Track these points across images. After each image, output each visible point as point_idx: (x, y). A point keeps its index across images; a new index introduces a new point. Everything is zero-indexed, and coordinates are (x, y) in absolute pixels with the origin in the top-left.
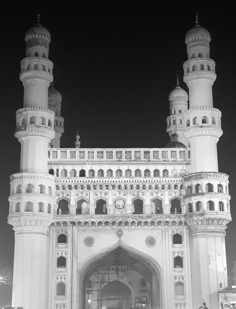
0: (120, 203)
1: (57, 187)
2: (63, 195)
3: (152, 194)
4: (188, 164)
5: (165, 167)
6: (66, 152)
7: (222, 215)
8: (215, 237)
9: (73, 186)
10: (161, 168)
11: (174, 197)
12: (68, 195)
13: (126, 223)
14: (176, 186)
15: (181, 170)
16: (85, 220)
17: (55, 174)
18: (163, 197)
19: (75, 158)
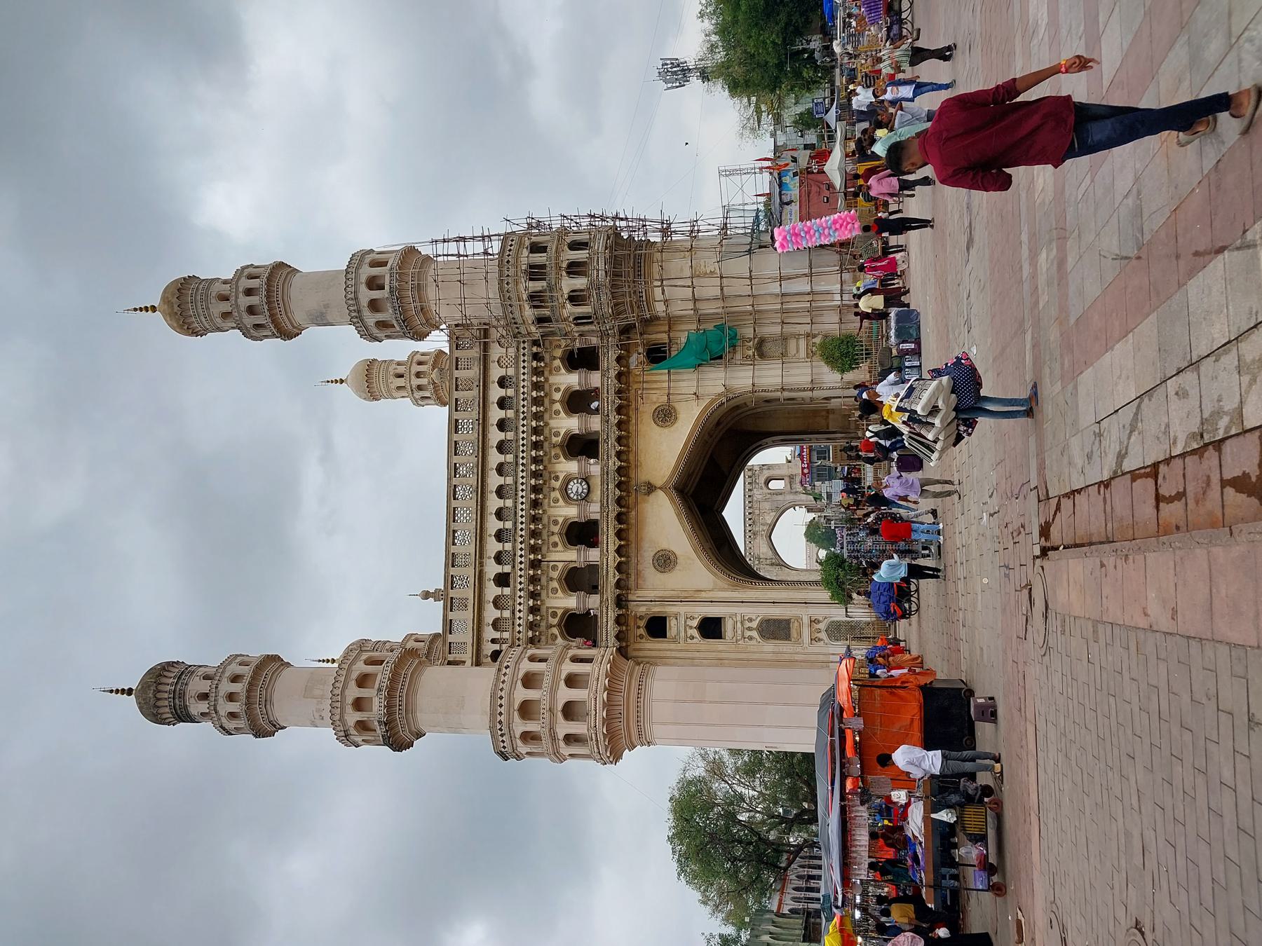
0: (575, 488)
1: (532, 641)
3: (557, 413)
9: (531, 602)
10: (496, 393)
12: (554, 615)
14: (536, 357)
16: (611, 570)
17: (504, 647)
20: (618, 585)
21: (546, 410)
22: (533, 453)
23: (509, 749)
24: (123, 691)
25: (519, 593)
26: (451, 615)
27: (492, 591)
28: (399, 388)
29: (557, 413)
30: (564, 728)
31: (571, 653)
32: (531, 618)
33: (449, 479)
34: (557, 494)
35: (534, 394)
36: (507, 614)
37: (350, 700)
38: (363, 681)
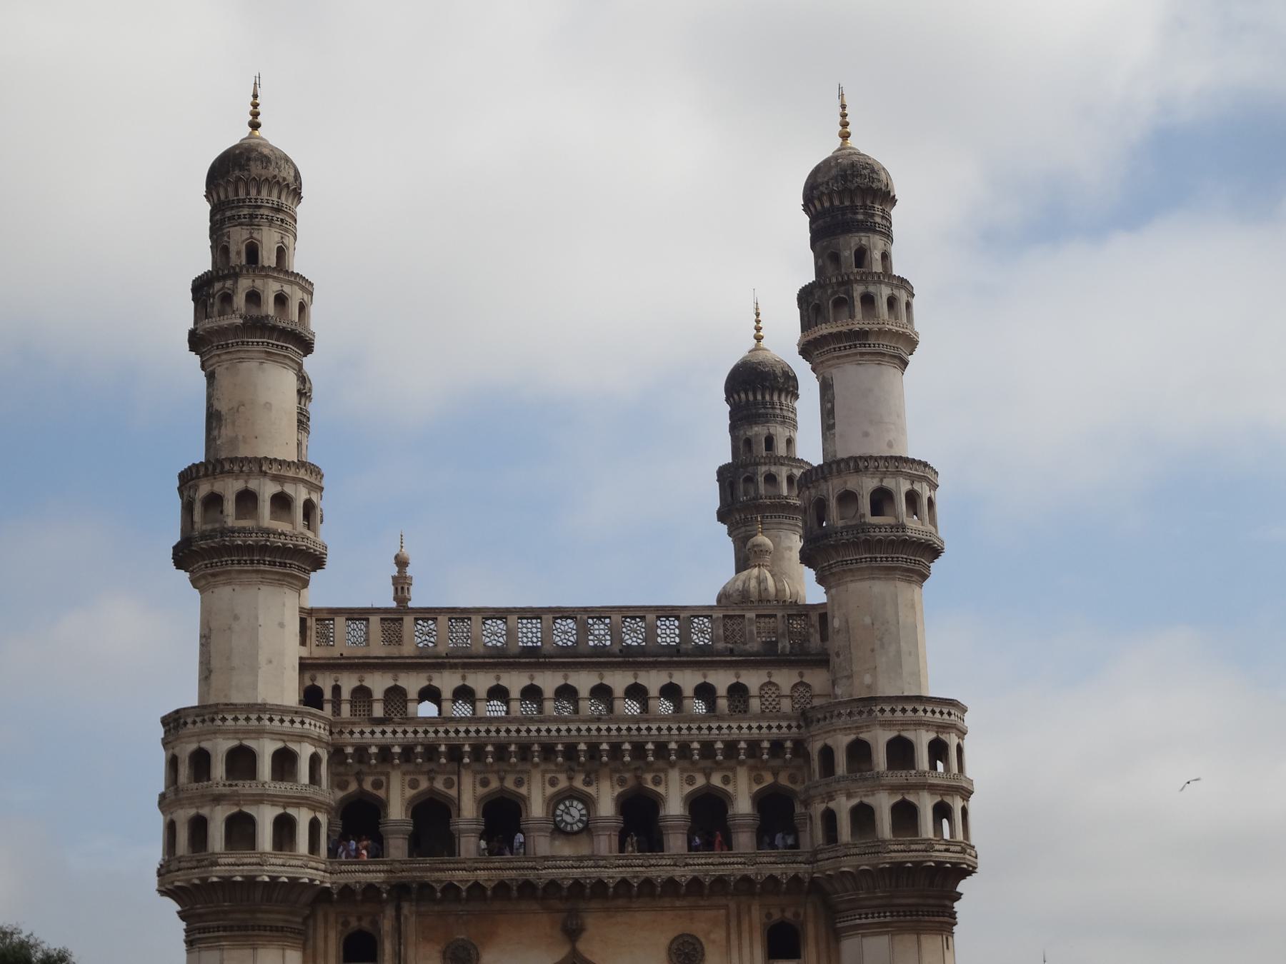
1: (337, 753)
2: (360, 785)
3: (691, 781)
4: (822, 661)
5: (738, 676)
6: (367, 620)
7: (947, 850)
8: (918, 929)
9: (397, 749)
11: (770, 786)
12: (377, 785)
13: (600, 883)
14: (777, 746)
15: (795, 685)
16: (446, 876)
17: (328, 708)
18: (729, 788)
19: (400, 643)
20: (425, 887)
21: (694, 763)
22: (627, 746)
23: (183, 732)
24: (255, 115)
25: (410, 729)
26: (375, 620)
27: (412, 683)
28: (748, 442)
29: (691, 781)
30: (218, 819)
31: (323, 818)
32: (374, 750)
33: (585, 610)
34: (563, 783)
35: (719, 745)
36: (378, 710)
37: (253, 485)
38: (282, 503)
